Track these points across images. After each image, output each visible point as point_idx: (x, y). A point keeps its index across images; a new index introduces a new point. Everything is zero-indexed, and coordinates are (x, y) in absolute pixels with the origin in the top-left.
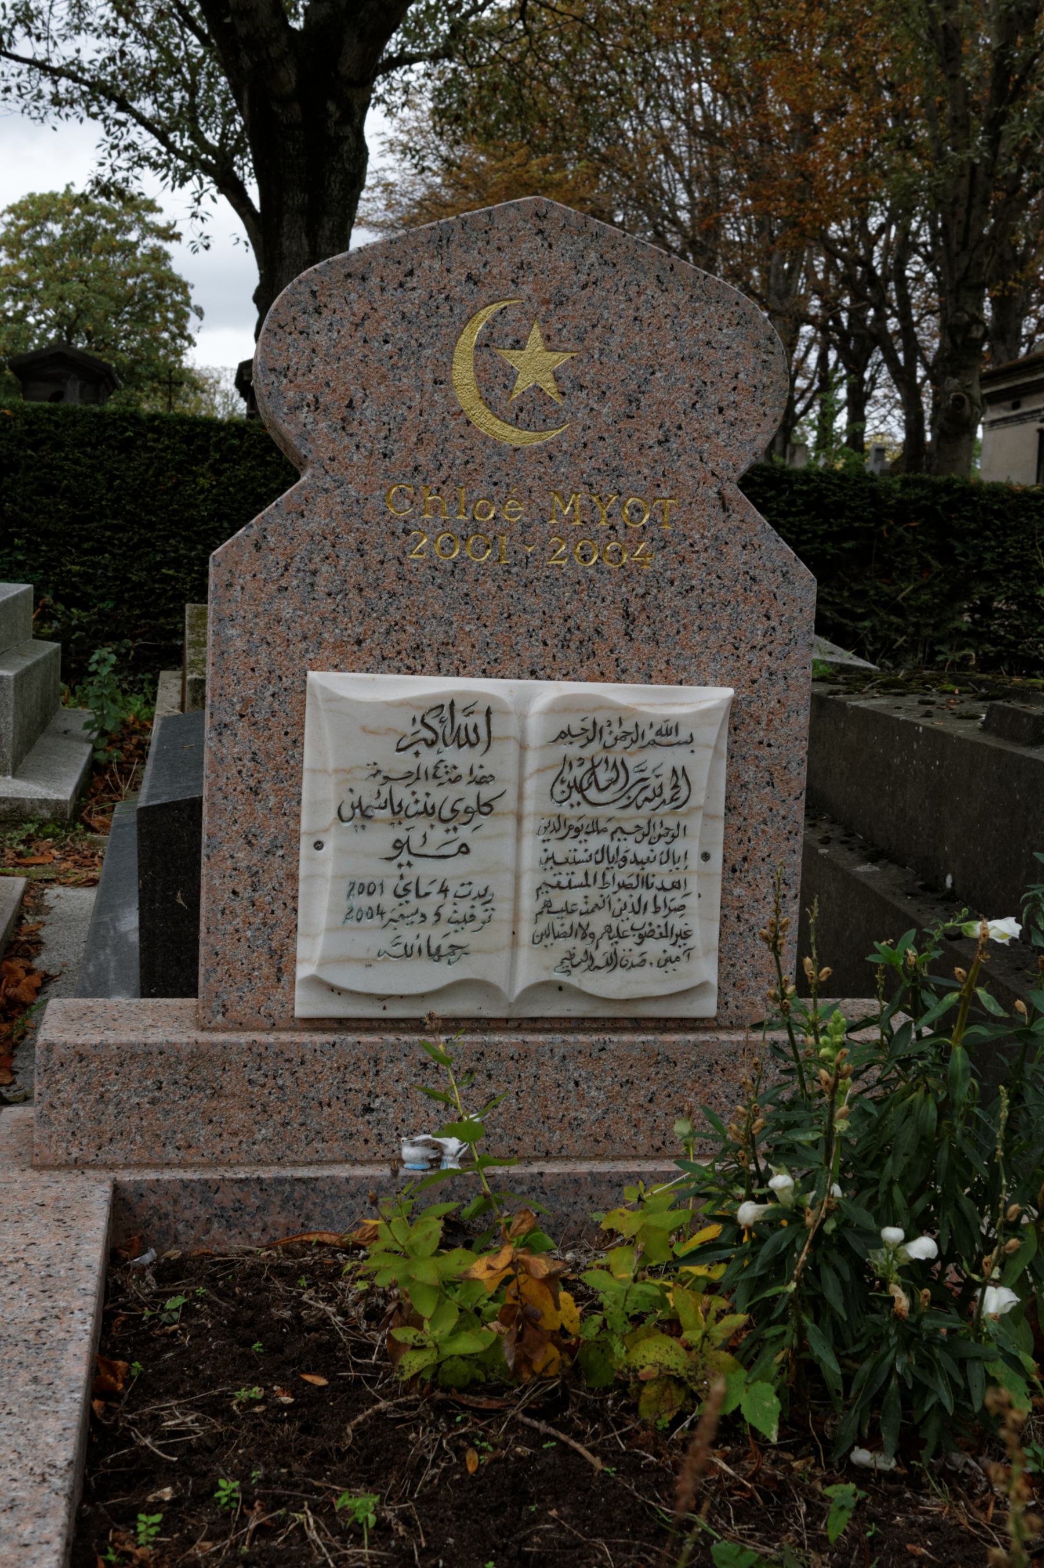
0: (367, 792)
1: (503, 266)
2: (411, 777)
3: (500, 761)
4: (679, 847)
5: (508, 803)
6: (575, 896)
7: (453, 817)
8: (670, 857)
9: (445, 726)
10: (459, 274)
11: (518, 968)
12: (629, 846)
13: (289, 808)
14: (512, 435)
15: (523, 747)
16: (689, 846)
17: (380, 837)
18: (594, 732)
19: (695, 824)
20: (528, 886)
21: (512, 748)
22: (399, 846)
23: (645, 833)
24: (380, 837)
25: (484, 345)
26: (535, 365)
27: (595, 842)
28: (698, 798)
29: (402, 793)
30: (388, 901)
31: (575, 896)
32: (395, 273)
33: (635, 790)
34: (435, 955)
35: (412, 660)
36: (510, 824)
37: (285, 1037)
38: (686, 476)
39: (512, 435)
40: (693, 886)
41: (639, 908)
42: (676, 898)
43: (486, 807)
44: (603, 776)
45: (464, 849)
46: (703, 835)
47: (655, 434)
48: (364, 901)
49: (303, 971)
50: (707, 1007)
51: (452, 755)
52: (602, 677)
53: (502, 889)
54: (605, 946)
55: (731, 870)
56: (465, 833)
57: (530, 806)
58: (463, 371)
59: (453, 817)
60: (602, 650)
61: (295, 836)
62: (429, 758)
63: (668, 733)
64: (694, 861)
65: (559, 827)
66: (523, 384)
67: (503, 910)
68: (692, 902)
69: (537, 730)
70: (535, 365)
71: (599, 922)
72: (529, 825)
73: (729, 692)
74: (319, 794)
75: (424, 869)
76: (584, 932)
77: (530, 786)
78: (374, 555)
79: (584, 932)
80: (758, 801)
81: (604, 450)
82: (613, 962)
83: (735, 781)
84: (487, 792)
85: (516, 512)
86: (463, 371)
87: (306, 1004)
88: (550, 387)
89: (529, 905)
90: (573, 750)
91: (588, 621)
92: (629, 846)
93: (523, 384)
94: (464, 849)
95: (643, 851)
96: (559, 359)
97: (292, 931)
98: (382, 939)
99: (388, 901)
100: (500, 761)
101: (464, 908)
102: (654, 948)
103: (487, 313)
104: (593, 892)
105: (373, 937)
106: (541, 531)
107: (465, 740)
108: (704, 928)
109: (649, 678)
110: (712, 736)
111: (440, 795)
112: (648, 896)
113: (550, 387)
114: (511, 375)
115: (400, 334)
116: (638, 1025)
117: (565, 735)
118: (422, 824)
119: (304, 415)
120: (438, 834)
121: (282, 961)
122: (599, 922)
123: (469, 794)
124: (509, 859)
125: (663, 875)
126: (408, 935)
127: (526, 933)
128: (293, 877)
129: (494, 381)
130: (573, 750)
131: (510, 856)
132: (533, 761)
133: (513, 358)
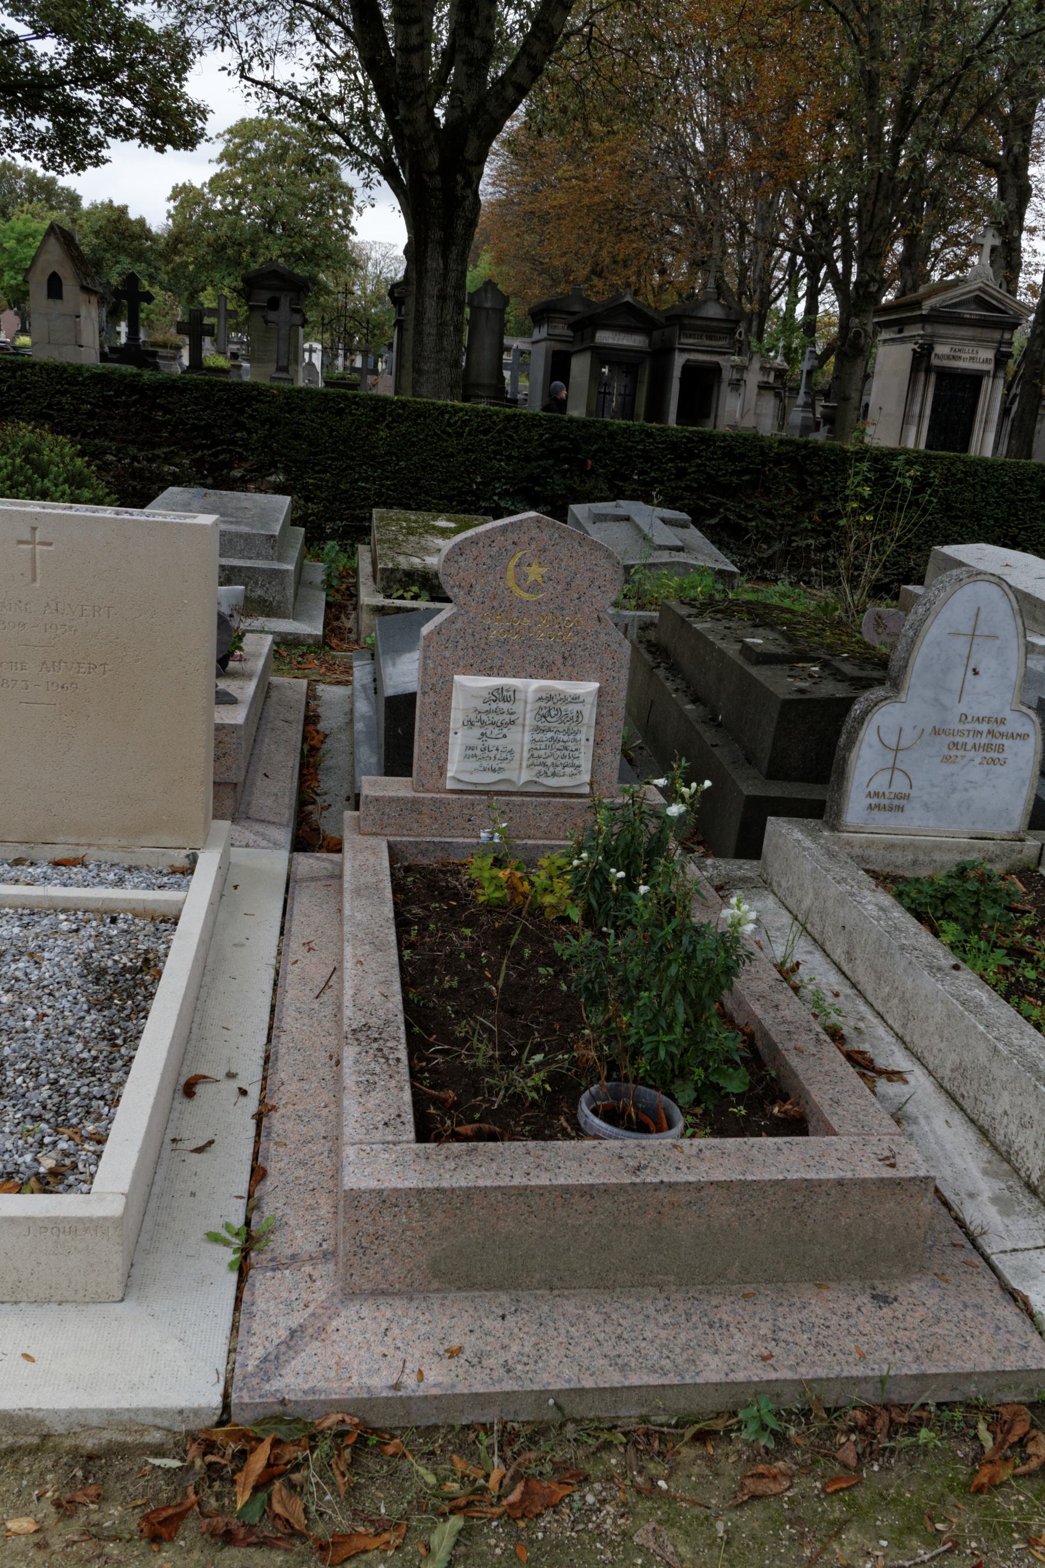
0: (473, 717)
1: (525, 538)
2: (488, 712)
3: (518, 707)
4: (578, 737)
5: (520, 721)
6: (542, 753)
7: (502, 725)
8: (575, 740)
9: (500, 695)
10: (510, 541)
11: (522, 776)
12: (561, 736)
13: (446, 719)
14: (526, 596)
15: (526, 702)
16: (582, 737)
17: (477, 732)
18: (550, 698)
19: (584, 729)
20: (526, 748)
21: (522, 703)
22: (482, 734)
23: (567, 732)
24: (477, 732)
25: (518, 565)
26: (535, 573)
27: (549, 735)
28: (585, 721)
29: (484, 717)
30: (478, 752)
31: (542, 753)
32: (488, 541)
33: (564, 718)
34: (494, 771)
35: (489, 672)
36: (520, 729)
37: (443, 795)
38: (586, 610)
39: (526, 596)
40: (583, 750)
41: (564, 757)
42: (576, 754)
43: (512, 722)
44: (553, 713)
45: (505, 736)
46: (587, 733)
47: (576, 596)
48: (470, 752)
49: (449, 774)
50: (586, 790)
51: (501, 705)
52: (554, 678)
53: (517, 750)
54: (552, 769)
55: (597, 744)
56: (505, 731)
57: (527, 722)
58: (510, 574)
59: (502, 725)
60: (555, 669)
61: (448, 729)
62: (494, 706)
63: (575, 699)
64: (583, 742)
65: (537, 729)
66: (531, 578)
67: (517, 756)
68: (582, 755)
69: (531, 697)
70: (535, 573)
71: (549, 761)
72: (527, 728)
73: (597, 685)
74: (456, 717)
75: (491, 742)
76: (544, 765)
77: (528, 716)
78: (478, 636)
79: (544, 765)
80: (607, 721)
81: (558, 601)
82: (554, 775)
83: (599, 715)
84: (513, 717)
85: (527, 622)
86: (510, 574)
87: (450, 785)
88: (540, 580)
89: (526, 755)
90: (543, 704)
91: (550, 659)
92: (561, 736)
93: (531, 578)
94: (505, 736)
95: (565, 738)
96: (544, 570)
97: (446, 760)
98: (477, 765)
99: (478, 752)
100: (518, 707)
101: (504, 755)
102: (568, 770)
103: (519, 555)
104: (548, 752)
105: (473, 764)
106: (535, 629)
107: (506, 700)
108: (585, 762)
109: (570, 679)
110: (592, 700)
111: (497, 718)
112: (566, 753)
113: (540, 580)
114: (526, 575)
115: (489, 562)
116: (562, 795)
117: (540, 699)
118: (491, 728)
119: (456, 590)
120: (496, 731)
121: (442, 771)
122: (549, 761)
123: (507, 718)
124: (519, 739)
125: (572, 746)
126: (485, 764)
127: (524, 764)
128: (447, 743)
129: (521, 578)
130: (543, 704)
131: (520, 739)
132: (529, 707)
133: (526, 569)
